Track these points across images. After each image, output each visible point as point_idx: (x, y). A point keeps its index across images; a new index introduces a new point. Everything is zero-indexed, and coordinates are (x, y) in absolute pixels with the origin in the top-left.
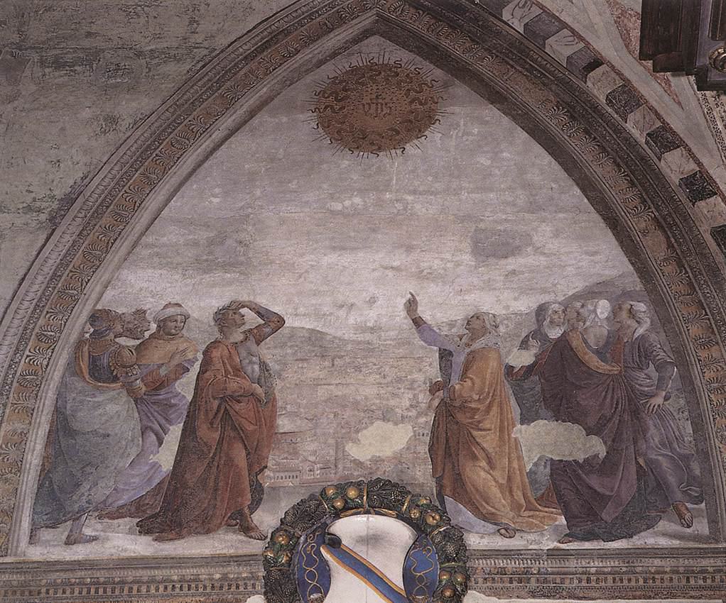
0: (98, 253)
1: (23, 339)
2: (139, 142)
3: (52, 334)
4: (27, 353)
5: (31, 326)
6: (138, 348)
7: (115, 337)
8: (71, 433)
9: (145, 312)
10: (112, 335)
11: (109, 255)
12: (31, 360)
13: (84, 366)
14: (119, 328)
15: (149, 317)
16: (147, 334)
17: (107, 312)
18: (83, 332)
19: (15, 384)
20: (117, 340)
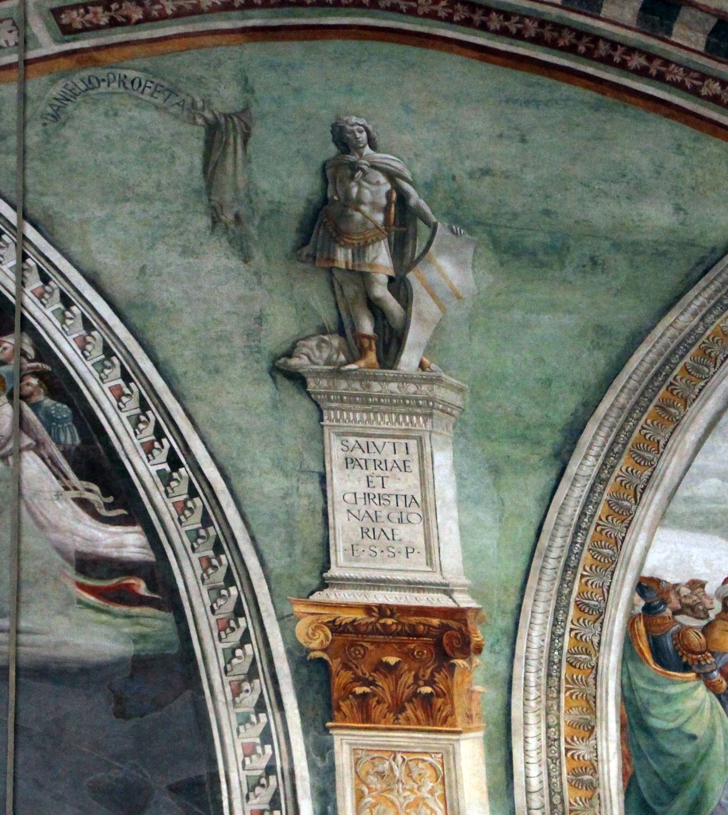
0: (626, 503)
1: (560, 607)
2: (646, 365)
3: (596, 603)
4: (569, 626)
5: (566, 591)
6: (707, 630)
7: (676, 612)
8: (648, 731)
9: (702, 585)
10: (668, 612)
11: (640, 508)
12: (576, 634)
13: (644, 644)
14: (675, 602)
15: (710, 589)
16: (712, 615)
17: (658, 581)
18: (632, 605)
19: (564, 663)
20: (679, 618)
